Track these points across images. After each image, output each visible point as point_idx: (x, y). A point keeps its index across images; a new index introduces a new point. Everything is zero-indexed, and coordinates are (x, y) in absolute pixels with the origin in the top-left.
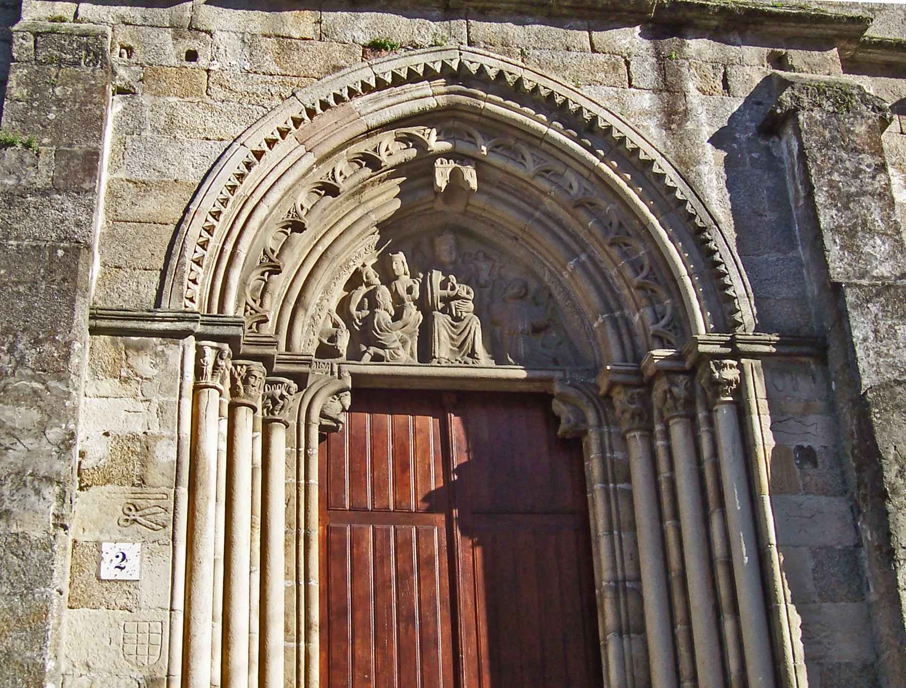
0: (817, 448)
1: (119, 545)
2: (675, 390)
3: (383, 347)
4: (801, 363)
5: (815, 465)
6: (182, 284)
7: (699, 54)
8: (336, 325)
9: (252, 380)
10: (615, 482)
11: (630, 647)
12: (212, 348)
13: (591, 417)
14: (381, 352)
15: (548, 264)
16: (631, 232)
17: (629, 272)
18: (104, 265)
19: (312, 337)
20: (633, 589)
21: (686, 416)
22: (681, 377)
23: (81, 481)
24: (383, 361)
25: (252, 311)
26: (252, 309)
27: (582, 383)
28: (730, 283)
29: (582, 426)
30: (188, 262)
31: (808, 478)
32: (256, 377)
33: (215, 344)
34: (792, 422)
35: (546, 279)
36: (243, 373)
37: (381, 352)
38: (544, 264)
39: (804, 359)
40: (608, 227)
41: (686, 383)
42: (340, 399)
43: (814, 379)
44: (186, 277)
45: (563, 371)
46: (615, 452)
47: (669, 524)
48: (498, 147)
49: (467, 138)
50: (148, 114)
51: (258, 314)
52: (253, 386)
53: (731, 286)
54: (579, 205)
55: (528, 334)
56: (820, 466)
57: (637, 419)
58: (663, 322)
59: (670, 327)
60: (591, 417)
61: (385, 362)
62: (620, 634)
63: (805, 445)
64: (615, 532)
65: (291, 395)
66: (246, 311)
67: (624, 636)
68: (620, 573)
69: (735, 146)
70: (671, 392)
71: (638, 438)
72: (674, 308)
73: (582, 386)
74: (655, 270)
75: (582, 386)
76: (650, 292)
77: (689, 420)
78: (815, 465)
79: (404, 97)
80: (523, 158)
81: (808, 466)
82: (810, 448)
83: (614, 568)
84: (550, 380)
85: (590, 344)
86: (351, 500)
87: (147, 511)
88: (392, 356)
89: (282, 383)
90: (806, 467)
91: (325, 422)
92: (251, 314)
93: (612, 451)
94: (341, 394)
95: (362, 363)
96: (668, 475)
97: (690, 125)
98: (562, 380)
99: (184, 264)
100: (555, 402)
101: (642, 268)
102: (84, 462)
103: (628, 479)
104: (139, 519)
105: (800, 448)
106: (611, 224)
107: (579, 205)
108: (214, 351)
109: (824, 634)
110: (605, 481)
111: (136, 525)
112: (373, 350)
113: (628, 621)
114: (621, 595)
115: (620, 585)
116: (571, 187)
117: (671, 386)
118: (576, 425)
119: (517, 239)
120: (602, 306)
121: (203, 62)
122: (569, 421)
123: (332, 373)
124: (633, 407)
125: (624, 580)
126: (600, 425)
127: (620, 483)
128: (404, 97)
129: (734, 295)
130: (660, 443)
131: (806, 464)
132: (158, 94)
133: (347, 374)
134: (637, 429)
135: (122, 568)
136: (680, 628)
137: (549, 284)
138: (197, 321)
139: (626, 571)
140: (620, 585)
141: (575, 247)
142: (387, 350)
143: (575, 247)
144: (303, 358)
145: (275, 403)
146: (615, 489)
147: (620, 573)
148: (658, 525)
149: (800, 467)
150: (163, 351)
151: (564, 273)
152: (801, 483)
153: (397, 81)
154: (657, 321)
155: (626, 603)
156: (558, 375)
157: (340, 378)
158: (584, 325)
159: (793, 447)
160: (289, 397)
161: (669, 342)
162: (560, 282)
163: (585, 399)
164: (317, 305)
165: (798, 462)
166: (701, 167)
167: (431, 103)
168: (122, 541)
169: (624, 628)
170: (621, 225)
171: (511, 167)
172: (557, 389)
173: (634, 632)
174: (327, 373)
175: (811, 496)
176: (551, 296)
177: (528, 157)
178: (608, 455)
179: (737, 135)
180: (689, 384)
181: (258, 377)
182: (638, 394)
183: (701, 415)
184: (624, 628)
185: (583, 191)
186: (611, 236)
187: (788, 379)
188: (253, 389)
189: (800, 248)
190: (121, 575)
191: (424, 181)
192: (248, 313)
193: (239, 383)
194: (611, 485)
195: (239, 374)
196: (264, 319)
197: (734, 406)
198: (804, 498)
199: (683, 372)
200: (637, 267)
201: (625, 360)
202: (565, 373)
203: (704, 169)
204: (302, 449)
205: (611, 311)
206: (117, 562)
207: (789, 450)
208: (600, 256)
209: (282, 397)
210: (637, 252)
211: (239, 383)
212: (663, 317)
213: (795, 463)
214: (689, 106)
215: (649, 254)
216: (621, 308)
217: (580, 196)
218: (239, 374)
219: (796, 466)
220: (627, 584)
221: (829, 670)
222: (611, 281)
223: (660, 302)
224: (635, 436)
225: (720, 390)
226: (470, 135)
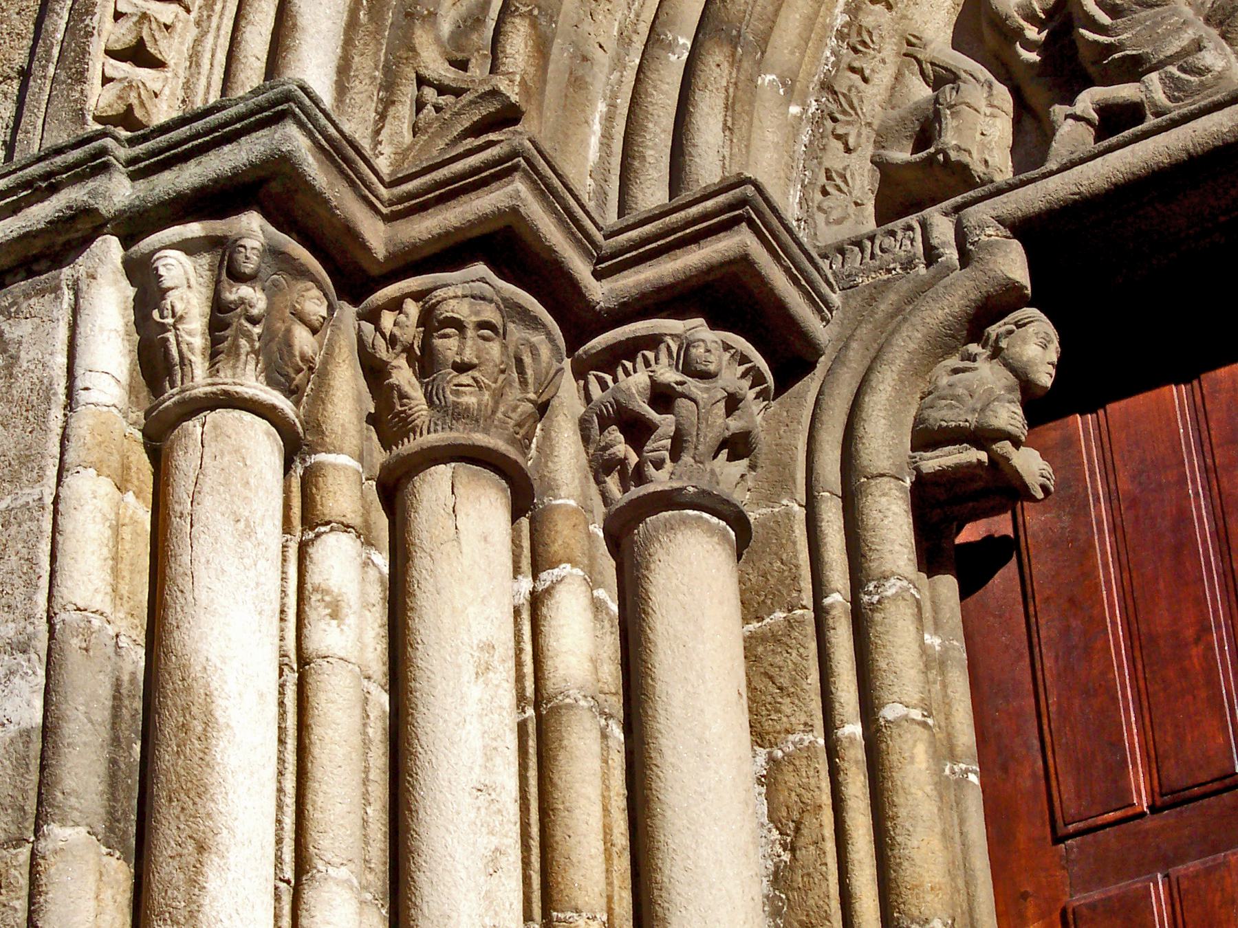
3: (1134, 69)
6: (80, 77)
8: (942, 78)
9: (448, 346)
12: (189, 247)
14: (1126, 92)
19: (835, 157)
24: (1141, 119)
25: (442, 100)
26: (442, 90)
32: (459, 325)
33: (195, 229)
36: (410, 331)
37: (1126, 92)
42: (997, 353)
44: (97, 47)
51: (467, 97)
52: (462, 368)
61: (1151, 122)
65: (705, 376)
66: (420, 105)
86: (1154, 759)
88: (1175, 88)
89: (653, 341)
91: (936, 461)
92: (438, 109)
94: (994, 330)
95: (1052, 165)
108: (205, 259)
112: (1087, 101)
123: (931, 256)
133: (993, 233)
138: (105, 168)
142: (1154, 76)
144: (709, 204)
145: (637, 431)
157: (965, 258)
160: (694, 386)
164: (841, 36)
174: (908, 265)
181: (470, 320)
188: (465, 379)
192: (429, 111)
193: (403, 375)
195: (392, 341)
196: (492, 107)
204: (838, 599)
209: (662, 397)
211: (403, 375)
218: (392, 341)
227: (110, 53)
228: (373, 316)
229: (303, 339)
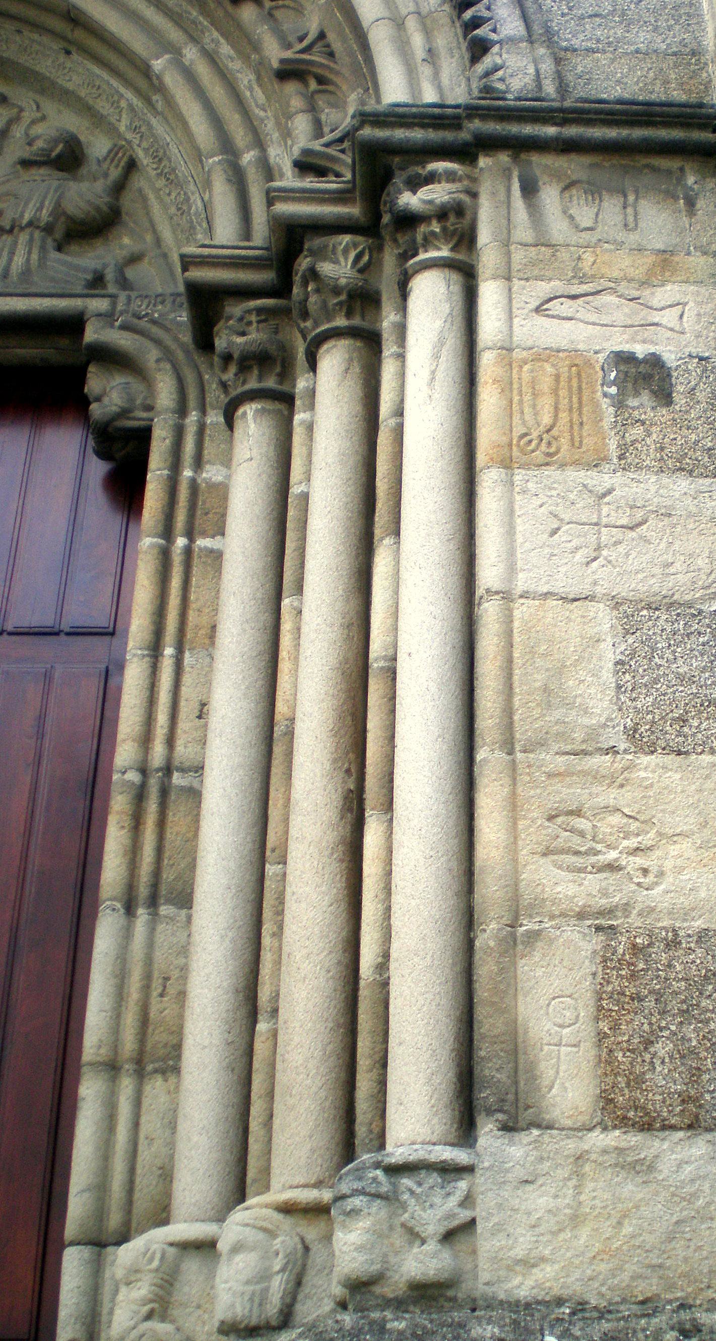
0: (670, 358)
2: (326, 268)
5: (665, 396)
10: (190, 535)
11: (150, 944)
21: (352, 333)
22: (346, 238)
27: (154, 322)
28: (486, 14)
31: (637, 432)
34: (608, 299)
35: (122, 129)
38: (122, 96)
41: (358, 257)
45: (113, 297)
46: (208, 467)
53: (490, 19)
55: (48, 229)
56: (680, 400)
58: (327, 138)
62: (130, 909)
63: (640, 350)
64: (169, 651)
67: (141, 911)
68: (158, 750)
71: (250, 415)
73: (155, 330)
74: (331, 37)
75: (155, 330)
76: (313, 85)
77: (359, 344)
78: (665, 396)
82: (655, 361)
83: (146, 739)
90: (632, 402)
93: (198, 462)
105: (623, 359)
109: (632, 843)
110: (168, 533)
113: (157, 873)
114: (152, 807)
115: (154, 784)
119: (68, 53)
120: (212, 139)
125: (168, 769)
126: (182, 410)
127: (204, 534)
129: (494, 37)
131: (637, 394)
137: (129, 136)
139: (180, 749)
140: (154, 784)
143: (174, 34)
146: (188, 552)
147: (158, 750)
149: (619, 404)
151: (154, 98)
152: (612, 445)
155: (161, 824)
156: (98, 305)
158: (190, 208)
159: (601, 357)
165: (613, 390)
169: (143, 891)
173: (169, 901)
175: (642, 476)
176: (132, 166)
178: (187, 473)
180: (366, 258)
182: (259, 311)
184: (143, 891)
187: (611, 207)
198: (619, 479)
202: (114, 305)
205: (227, 146)
207: (589, 364)
212: (332, 131)
219: (605, 403)
221: (635, 949)
222: (248, 94)
224: (245, 413)
225: (419, 238)
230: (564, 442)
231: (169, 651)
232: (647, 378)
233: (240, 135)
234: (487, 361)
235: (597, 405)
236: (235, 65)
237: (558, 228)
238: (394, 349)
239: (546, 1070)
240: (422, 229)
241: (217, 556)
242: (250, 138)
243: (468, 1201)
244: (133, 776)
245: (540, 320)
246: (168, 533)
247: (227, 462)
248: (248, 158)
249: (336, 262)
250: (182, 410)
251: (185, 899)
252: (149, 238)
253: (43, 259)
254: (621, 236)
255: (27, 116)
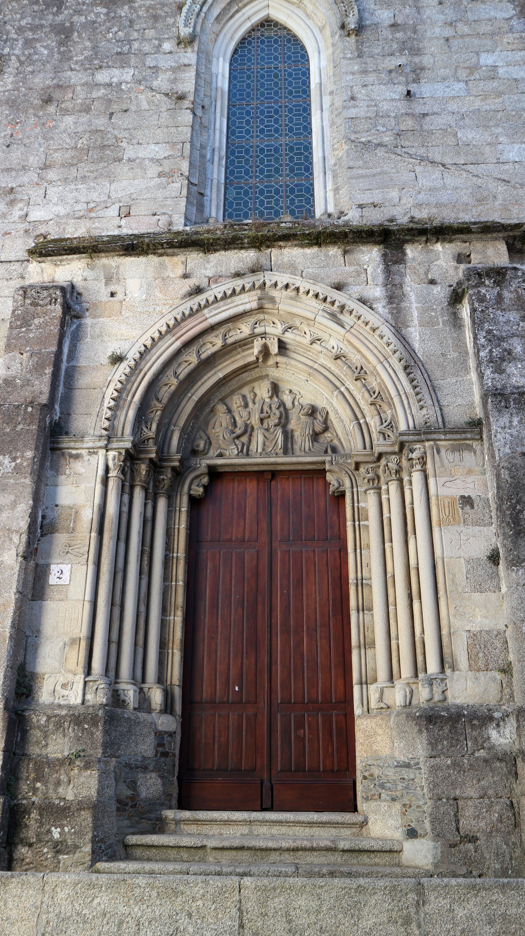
1: (60, 566)
4: (467, 444)
5: (472, 507)
6: (101, 421)
7: (413, 259)
10: (359, 521)
13: (347, 483)
15: (325, 394)
16: (368, 372)
17: (367, 395)
18: (61, 413)
20: (368, 584)
21: (397, 480)
22: (394, 456)
23: (41, 532)
29: (342, 489)
30: (105, 408)
39: (468, 442)
40: (355, 370)
43: (475, 453)
47: (387, 545)
48: (290, 328)
49: (272, 325)
50: (89, 329)
54: (337, 358)
56: (476, 507)
57: (371, 482)
58: (385, 424)
59: (389, 427)
60: (347, 483)
64: (358, 551)
69: (433, 314)
70: (387, 465)
72: (392, 415)
74: (381, 393)
78: (472, 507)
79: (233, 305)
80: (305, 333)
81: (468, 508)
82: (469, 497)
84: (324, 463)
85: (349, 440)
87: (76, 547)
90: (465, 508)
93: (358, 502)
96: (388, 515)
97: (403, 305)
98: (331, 462)
99: (103, 410)
100: (328, 474)
101: (374, 393)
102: (45, 522)
103: (367, 519)
104: (71, 551)
105: (463, 497)
106: (356, 368)
107: (337, 358)
110: (354, 521)
111: (69, 554)
115: (359, 582)
116: (333, 348)
117: (388, 462)
118: (338, 488)
121: (120, 296)
122: (334, 485)
124: (369, 475)
126: (352, 487)
127: (362, 521)
128: (233, 305)
129: (426, 405)
130: (384, 497)
132: (95, 317)
134: (371, 489)
135: (60, 578)
136: (391, 608)
140: (359, 582)
141: (338, 384)
146: (359, 525)
148: (382, 546)
149: (462, 509)
150: (89, 460)
153: (225, 297)
154: (382, 424)
156: (328, 458)
159: (458, 497)
161: (388, 436)
162: (332, 405)
163: (344, 472)
166: (409, 329)
167: (248, 307)
168: (61, 563)
170: (362, 368)
171: (298, 338)
172: (327, 467)
177: (308, 332)
178: (356, 505)
179: (435, 307)
183: (406, 478)
185: (339, 349)
186: (356, 375)
187: (457, 454)
189: (472, 373)
190: (60, 582)
191: (250, 351)
194: (357, 523)
197: (422, 473)
199: (394, 453)
200: (370, 392)
201: (365, 448)
203: (411, 330)
205: (357, 419)
206: (58, 575)
207: (455, 499)
208: (351, 388)
210: (372, 384)
213: (458, 506)
214: (405, 292)
215: (379, 384)
216: (364, 417)
217: (338, 353)
220: (364, 581)
223: (384, 412)
226: (274, 323)
227: (106, 418)
228: (134, 464)
229: (126, 468)
230: (452, 520)
231: (358, 551)
232: (468, 502)
233: (359, 416)
234: (433, 500)
235: (458, 509)
236: (355, 393)
237: (446, 462)
238: (408, 487)
239: (459, 660)
240: (414, 462)
241: (367, 527)
242: (361, 415)
243: (446, 685)
244: (355, 581)
245: (444, 488)
246: (354, 521)
247: (366, 501)
248: (361, 421)
249: (392, 462)
250: (352, 487)
251: (371, 609)
252: (335, 434)
253: (313, 445)
254: (460, 464)
255: (298, 397)
